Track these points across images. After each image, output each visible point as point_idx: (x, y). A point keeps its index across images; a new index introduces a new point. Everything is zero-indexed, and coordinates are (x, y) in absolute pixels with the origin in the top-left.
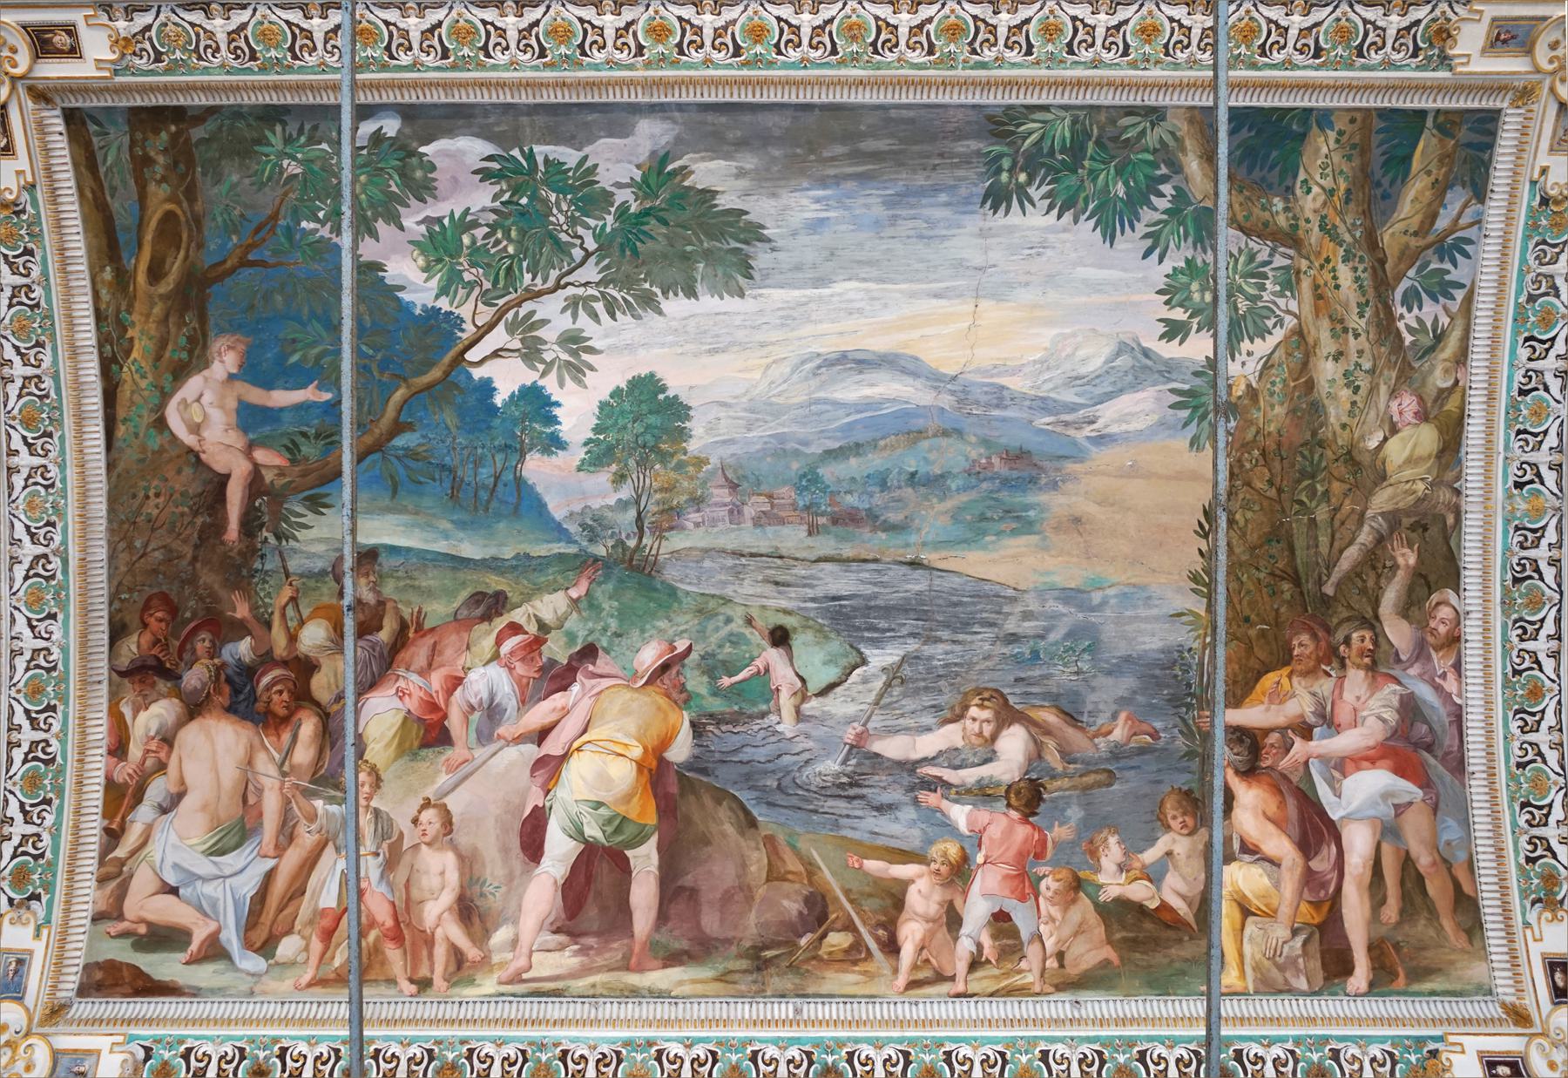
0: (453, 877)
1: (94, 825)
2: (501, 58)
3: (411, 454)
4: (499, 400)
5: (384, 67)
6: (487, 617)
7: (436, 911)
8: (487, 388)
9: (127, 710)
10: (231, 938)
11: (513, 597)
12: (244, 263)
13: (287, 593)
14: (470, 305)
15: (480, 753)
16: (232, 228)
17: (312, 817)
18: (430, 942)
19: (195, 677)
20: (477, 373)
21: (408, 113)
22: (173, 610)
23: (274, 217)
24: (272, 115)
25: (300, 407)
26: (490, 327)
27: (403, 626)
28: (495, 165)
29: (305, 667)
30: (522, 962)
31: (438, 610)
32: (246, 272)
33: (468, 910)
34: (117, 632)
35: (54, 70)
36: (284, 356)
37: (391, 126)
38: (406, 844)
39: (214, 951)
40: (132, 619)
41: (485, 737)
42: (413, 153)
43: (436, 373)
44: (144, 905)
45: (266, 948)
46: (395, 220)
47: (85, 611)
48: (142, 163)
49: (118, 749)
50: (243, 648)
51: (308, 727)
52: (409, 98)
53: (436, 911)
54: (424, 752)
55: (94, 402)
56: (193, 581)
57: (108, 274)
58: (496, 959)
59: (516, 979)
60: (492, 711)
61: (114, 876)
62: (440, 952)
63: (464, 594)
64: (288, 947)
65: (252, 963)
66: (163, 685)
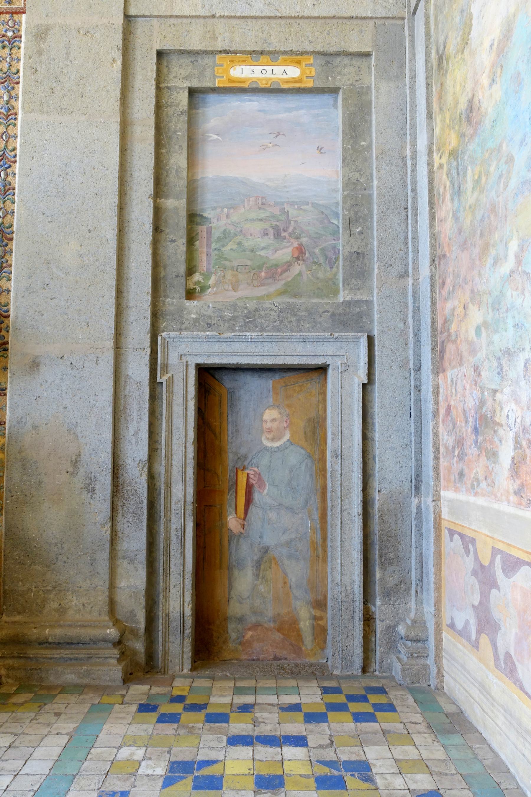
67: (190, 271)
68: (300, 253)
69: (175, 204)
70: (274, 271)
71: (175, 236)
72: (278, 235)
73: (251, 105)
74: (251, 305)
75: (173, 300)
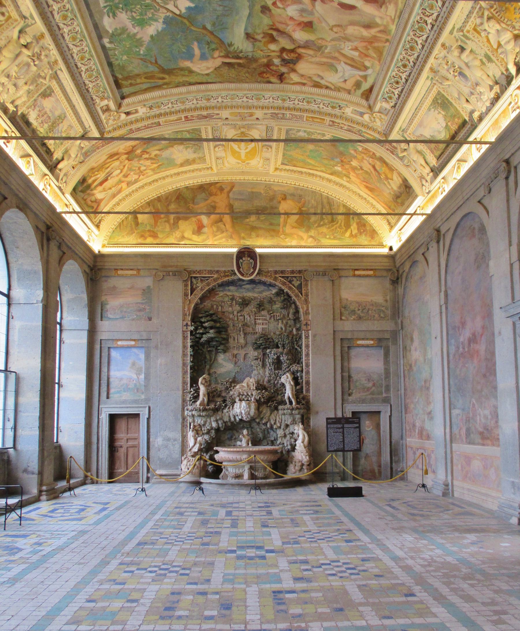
0: (356, 28)
1: (324, 91)
2: (78, 28)
3: (214, 25)
4: (192, 5)
5: (90, 52)
6: (270, 10)
7: (365, 33)
8: (189, 9)
9: (292, 82)
10: (362, 73)
11: (263, 3)
13: (259, 52)
14: (160, 14)
15: (316, 15)
16: (147, 67)
17: (330, 53)
18: (375, 37)
19: (284, 70)
20: (184, 11)
21: (100, 38)
22: (264, 72)
23: (141, 59)
25: (200, 48)
26: (167, 9)
27: (272, 29)
28: (111, 15)
29: (283, 50)
30: (388, 18)
31: (266, 21)
32: (159, 62)
33: (368, 26)
34: (270, 82)
36: (184, 53)
38: (343, 36)
39: (365, 77)
40: (265, 80)
41: (312, 13)
43: (185, 21)
44: (349, 85)
45: (366, 68)
46: (135, 35)
47: (263, 90)
48: (131, 85)
49: (304, 84)
50: (277, 61)
51: (301, 51)
52: (96, 39)
53: (365, 33)
54: (314, 27)
55: (203, 87)
56: (255, 69)
57: (165, 86)
58: (385, 23)
59: (393, 21)
60: (302, 11)
61: (338, 89)
62: (379, 35)
63: (261, 15)
64: (367, 64)
65: (369, 71)
66: (286, 75)
67: (349, 389)
68: (374, 385)
69: (346, 374)
70: (368, 389)
71: (346, 381)
72: (369, 380)
73: (362, 349)
74: (364, 397)
75: (346, 397)
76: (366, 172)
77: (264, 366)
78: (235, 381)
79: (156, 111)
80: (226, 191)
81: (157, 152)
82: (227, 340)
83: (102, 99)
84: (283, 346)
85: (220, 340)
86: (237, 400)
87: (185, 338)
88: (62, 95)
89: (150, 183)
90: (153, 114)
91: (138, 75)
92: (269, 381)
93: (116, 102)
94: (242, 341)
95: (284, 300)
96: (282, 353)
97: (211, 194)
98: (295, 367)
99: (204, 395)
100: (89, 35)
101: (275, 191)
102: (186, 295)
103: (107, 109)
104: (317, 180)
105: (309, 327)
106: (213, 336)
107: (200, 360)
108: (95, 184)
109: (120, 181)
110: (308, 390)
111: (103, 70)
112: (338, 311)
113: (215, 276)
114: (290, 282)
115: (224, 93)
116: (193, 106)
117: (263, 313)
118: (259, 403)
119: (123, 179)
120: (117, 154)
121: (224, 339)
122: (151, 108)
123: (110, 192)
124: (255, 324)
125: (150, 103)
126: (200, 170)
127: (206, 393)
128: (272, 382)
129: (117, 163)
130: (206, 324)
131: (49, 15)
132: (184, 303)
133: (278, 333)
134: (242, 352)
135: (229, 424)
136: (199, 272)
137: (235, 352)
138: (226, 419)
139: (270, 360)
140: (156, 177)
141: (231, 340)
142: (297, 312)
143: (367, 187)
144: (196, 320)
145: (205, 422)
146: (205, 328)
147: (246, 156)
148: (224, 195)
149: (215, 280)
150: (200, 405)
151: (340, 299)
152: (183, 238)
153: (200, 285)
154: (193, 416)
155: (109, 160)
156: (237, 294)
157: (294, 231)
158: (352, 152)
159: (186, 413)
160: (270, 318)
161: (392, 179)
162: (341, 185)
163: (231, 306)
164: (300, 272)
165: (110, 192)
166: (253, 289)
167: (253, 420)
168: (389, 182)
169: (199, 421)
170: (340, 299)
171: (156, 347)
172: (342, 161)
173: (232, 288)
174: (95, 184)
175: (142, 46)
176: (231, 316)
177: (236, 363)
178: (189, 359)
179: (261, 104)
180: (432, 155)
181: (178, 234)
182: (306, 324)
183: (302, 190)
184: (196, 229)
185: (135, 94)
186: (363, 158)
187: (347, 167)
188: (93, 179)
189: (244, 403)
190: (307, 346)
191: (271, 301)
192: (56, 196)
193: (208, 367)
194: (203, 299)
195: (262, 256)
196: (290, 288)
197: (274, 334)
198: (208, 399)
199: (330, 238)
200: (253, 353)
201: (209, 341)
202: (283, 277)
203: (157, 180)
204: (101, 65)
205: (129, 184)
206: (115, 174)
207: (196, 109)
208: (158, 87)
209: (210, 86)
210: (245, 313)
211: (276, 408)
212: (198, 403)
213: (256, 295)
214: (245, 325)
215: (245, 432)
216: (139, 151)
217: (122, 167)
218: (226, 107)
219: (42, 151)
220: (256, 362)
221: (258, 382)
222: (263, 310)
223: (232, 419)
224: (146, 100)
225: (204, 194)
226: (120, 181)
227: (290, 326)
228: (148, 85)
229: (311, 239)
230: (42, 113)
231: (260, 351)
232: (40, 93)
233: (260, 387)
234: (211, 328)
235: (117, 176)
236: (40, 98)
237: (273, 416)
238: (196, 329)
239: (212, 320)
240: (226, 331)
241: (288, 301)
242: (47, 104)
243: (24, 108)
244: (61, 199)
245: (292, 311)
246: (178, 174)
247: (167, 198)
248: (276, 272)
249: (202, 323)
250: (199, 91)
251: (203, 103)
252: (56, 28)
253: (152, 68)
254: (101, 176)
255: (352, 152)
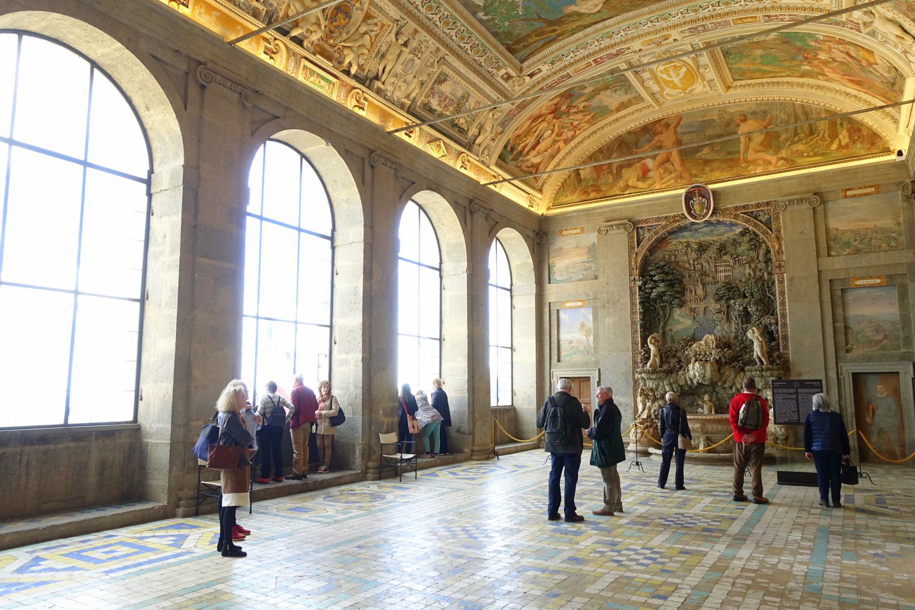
5: (468, 30)
12: (540, 18)
21: (474, 14)
24: (495, 35)
32: (542, 17)
35: (513, 73)
37: (481, 15)
42: (485, 6)
48: (525, 47)
52: (471, 17)
55: (599, 26)
67: (847, 344)
68: (886, 337)
69: (840, 325)
70: (877, 343)
71: (842, 333)
72: (877, 331)
73: (864, 291)
74: (870, 354)
75: (842, 354)
76: (842, 63)
77: (728, 319)
78: (694, 339)
79: (560, 65)
80: (672, 126)
81: (584, 104)
82: (683, 293)
83: (499, 69)
84: (752, 294)
85: (673, 293)
86: (693, 361)
87: (632, 294)
88: (456, 77)
89: (589, 136)
90: (557, 68)
91: (528, 36)
92: (736, 337)
93: (515, 67)
94: (700, 292)
95: (751, 240)
96: (749, 303)
97: (656, 133)
98: (767, 320)
99: (655, 356)
100: (461, 15)
101: (732, 114)
102: (631, 248)
103: (508, 78)
104: (785, 89)
105: (783, 270)
106: (663, 290)
107: (651, 317)
108: (527, 149)
109: (555, 142)
110: (786, 347)
111: (488, 41)
112: (823, 246)
113: (664, 223)
114: (756, 218)
115: (624, 25)
116: (597, 49)
117: (725, 258)
118: (719, 364)
119: (557, 138)
120: (541, 116)
121: (678, 292)
122: (553, 63)
123: (547, 154)
124: (717, 272)
125: (550, 59)
126: (640, 110)
127: (657, 353)
128: (739, 338)
129: (544, 124)
130: (656, 278)
131: (415, 11)
132: (630, 257)
133: (743, 280)
134: (701, 307)
135: (687, 388)
136: (646, 221)
137: (693, 306)
138: (682, 383)
139: (736, 313)
140: (594, 128)
141: (688, 293)
142: (768, 252)
143: (852, 81)
144: (646, 273)
145: (658, 386)
146: (655, 282)
147: (682, 83)
148: (671, 131)
149: (663, 228)
150: (651, 366)
151: (827, 229)
152: (627, 187)
153: (647, 235)
154: (643, 379)
155: (534, 124)
156: (692, 240)
157: (760, 155)
158: (813, 43)
159: (637, 375)
160: (735, 263)
161: (877, 64)
162: (818, 87)
163: (686, 254)
164: (768, 204)
165: (547, 154)
166: (712, 231)
167: (713, 384)
168: (874, 69)
169: (651, 384)
170: (827, 229)
171: (604, 307)
172: (806, 58)
173: (685, 234)
174: (527, 149)
175: (518, 7)
176: (687, 265)
177: (694, 318)
178: (638, 317)
179: (670, 24)
180: (907, 19)
181: (621, 184)
182: (779, 266)
183: (766, 104)
184: (641, 175)
185: (532, 54)
186: (830, 48)
187: (816, 62)
188: (522, 145)
189: (697, 364)
190: (782, 293)
191: (735, 243)
192: (478, 170)
193: (662, 324)
194: (652, 250)
195: (714, 192)
196: (755, 225)
197: (740, 281)
198: (661, 360)
199: (808, 156)
200: (714, 306)
201: (661, 296)
202: (746, 213)
203: (595, 132)
204: (485, 38)
205: (566, 142)
206: (545, 135)
207: (601, 50)
208: (554, 40)
209: (607, 22)
210: (702, 261)
211: (742, 370)
212: (648, 364)
213: (715, 238)
214: (704, 274)
215: (706, 397)
216: (564, 108)
217: (551, 127)
218: (633, 39)
219: (454, 133)
220: (720, 316)
221: (718, 340)
222: (725, 254)
223: (689, 382)
224: (545, 57)
225: (647, 136)
226: (555, 142)
227: (761, 270)
228: (543, 42)
229: (782, 162)
230: (443, 98)
231: (723, 302)
232: (433, 80)
233: (723, 344)
234: (663, 281)
235: (549, 136)
236: (436, 86)
237: (738, 379)
238: (645, 283)
239: (663, 272)
240: (681, 283)
241: (755, 243)
242: (446, 88)
243: (423, 98)
244: (487, 172)
245: (762, 252)
246: (617, 120)
247: (609, 148)
248: (737, 209)
249: (652, 276)
250: (596, 31)
251: (607, 42)
252: (425, 20)
253: (538, 25)
254: (531, 140)
255: (813, 43)
